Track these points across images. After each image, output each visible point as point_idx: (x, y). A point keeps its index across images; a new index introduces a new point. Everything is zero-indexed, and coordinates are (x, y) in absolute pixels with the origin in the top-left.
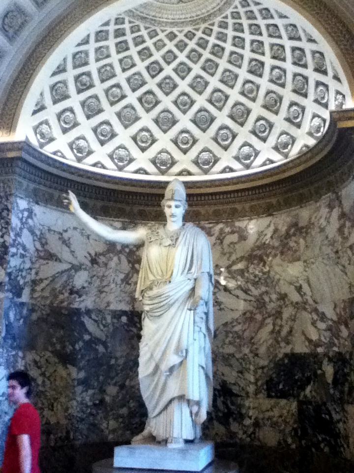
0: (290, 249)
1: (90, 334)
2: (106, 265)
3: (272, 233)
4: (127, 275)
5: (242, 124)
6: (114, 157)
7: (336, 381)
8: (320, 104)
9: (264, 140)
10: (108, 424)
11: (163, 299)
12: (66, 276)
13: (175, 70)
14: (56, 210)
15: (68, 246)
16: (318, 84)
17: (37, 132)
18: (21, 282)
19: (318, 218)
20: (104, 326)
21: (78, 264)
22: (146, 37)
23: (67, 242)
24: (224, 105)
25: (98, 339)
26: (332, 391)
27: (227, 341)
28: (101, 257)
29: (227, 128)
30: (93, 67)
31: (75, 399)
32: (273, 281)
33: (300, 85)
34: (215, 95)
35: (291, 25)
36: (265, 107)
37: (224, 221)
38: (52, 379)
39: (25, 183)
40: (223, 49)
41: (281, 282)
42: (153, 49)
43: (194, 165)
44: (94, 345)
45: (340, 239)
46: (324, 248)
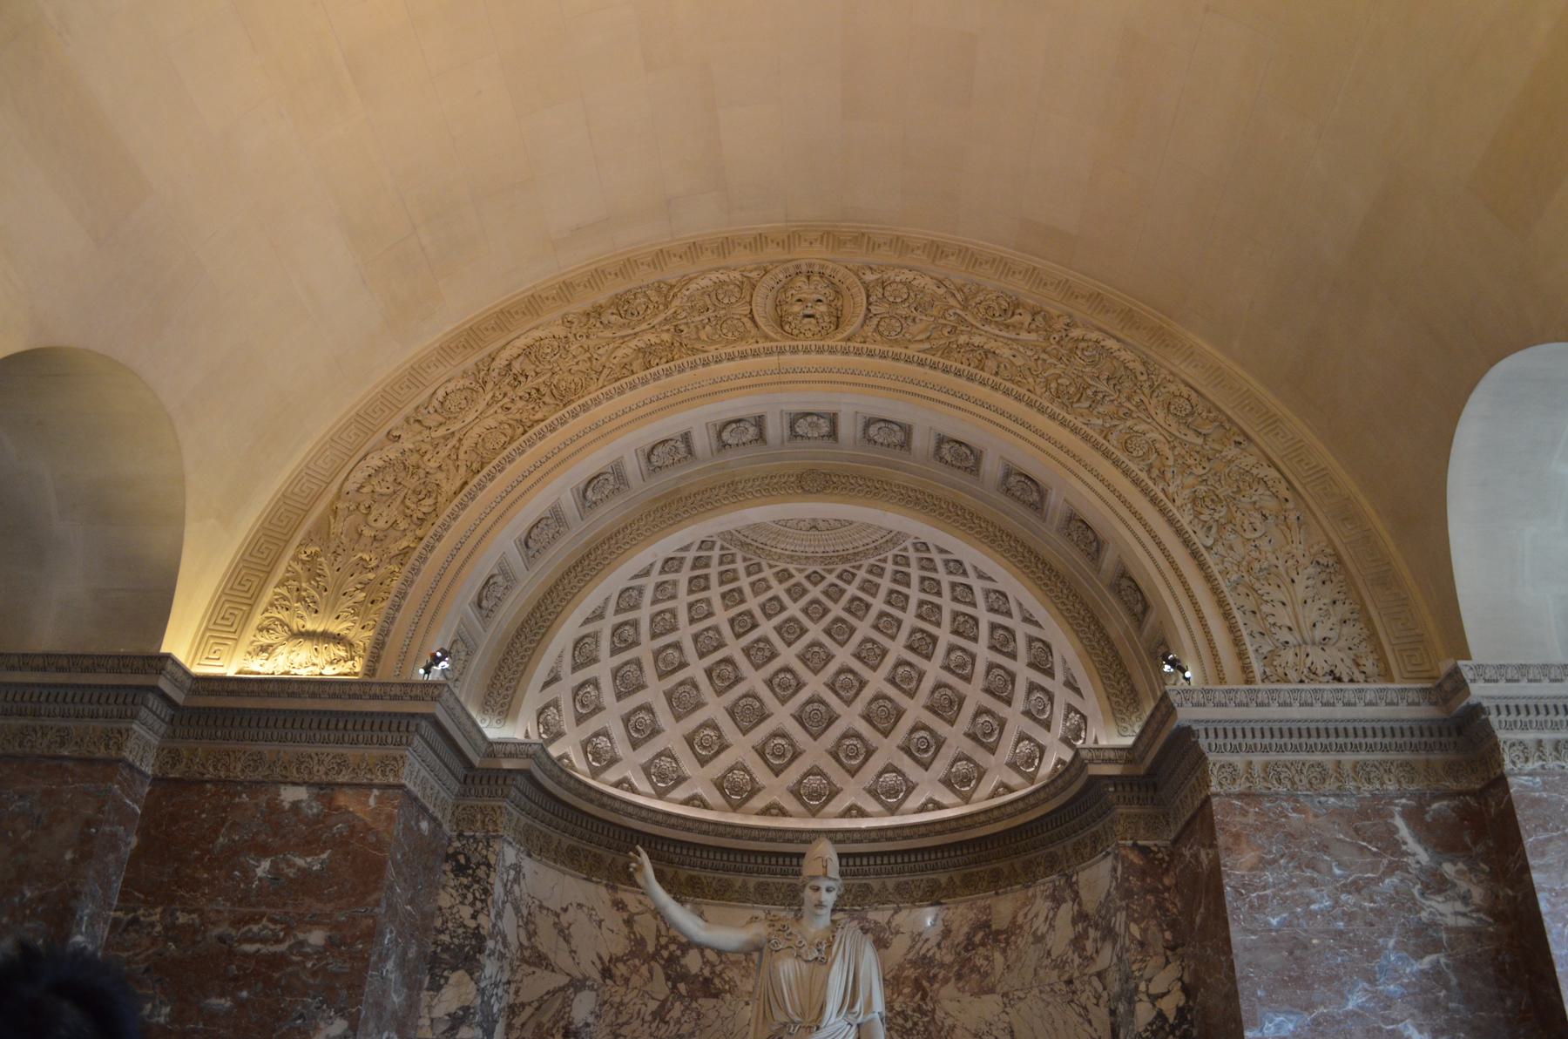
0: (975, 969)
2: (627, 981)
3: (940, 938)
4: (664, 1003)
5: (886, 734)
6: (653, 771)
8: (1034, 719)
9: (926, 766)
12: (560, 1001)
13: (778, 629)
14: (553, 868)
15: (567, 939)
16: (1033, 687)
17: (541, 720)
18: (495, 1010)
19: (1030, 917)
21: (580, 977)
22: (742, 573)
23: (567, 932)
24: (857, 694)
28: (620, 965)
29: (858, 736)
30: (644, 614)
32: (942, 1029)
33: (999, 682)
34: (842, 677)
35: (996, 591)
36: (931, 708)
37: (847, 908)
39: (516, 814)
40: (868, 606)
41: (958, 1031)
42: (747, 591)
43: (792, 797)
45: (1077, 961)
46: (1041, 972)
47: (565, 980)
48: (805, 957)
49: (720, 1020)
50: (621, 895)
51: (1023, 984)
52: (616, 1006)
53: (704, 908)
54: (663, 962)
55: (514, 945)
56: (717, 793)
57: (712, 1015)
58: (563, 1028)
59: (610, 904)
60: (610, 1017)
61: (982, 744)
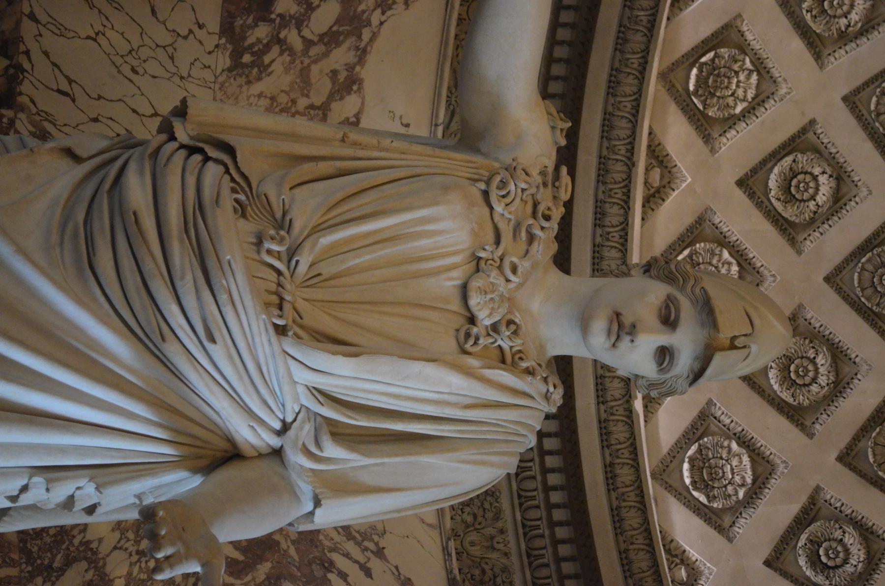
11: (190, 302)
43: (688, 220)
48: (476, 283)
49: (164, 38)
56: (705, 31)
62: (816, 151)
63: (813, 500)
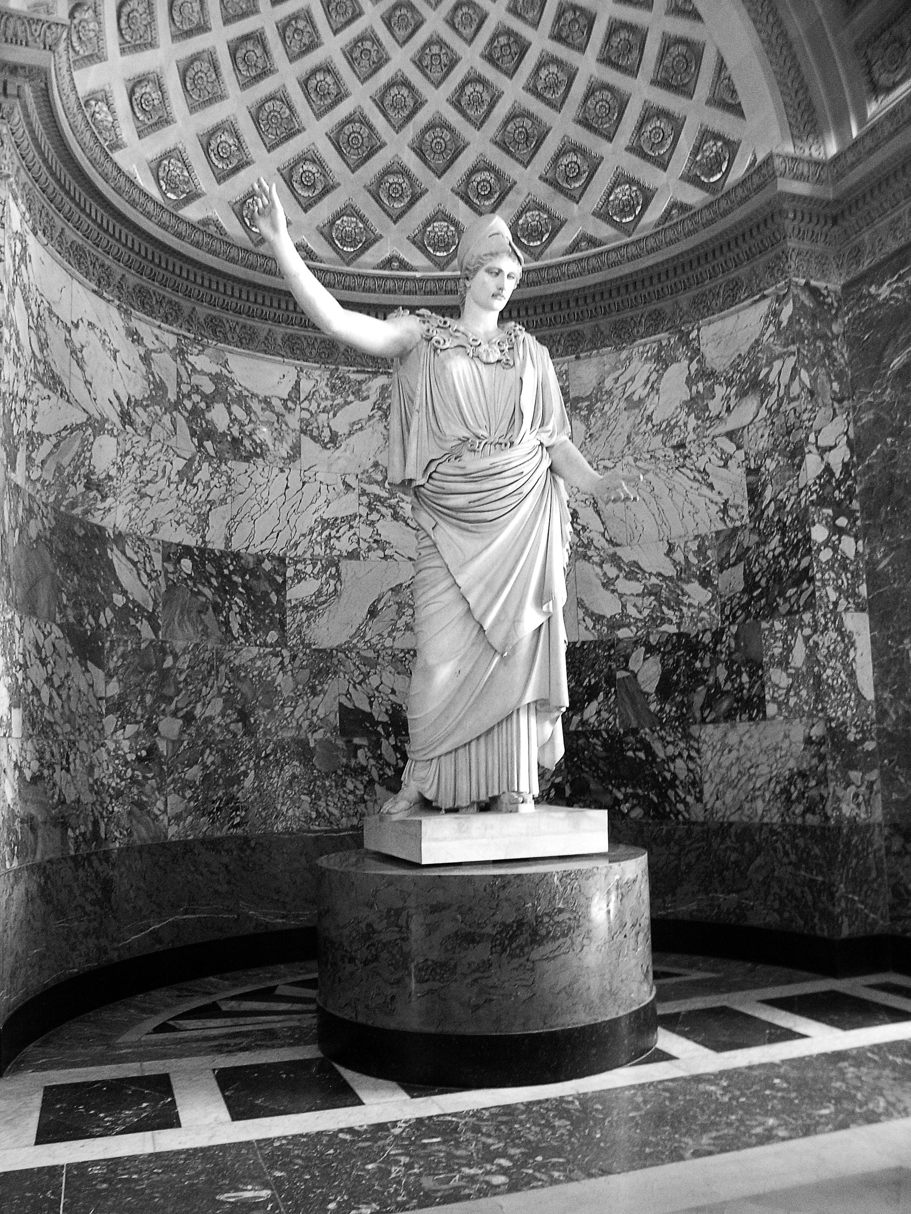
1: (124, 593)
2: (149, 430)
4: (191, 461)
6: (161, 174)
7: (665, 689)
8: (644, 156)
10: (166, 805)
15: (80, 364)
19: (622, 380)
20: (149, 575)
21: (99, 418)
23: (79, 355)
24: (409, 118)
25: (139, 606)
26: (654, 707)
27: (400, 624)
28: (139, 410)
29: (404, 172)
31: (103, 745)
36: (503, 146)
38: (64, 697)
44: (132, 622)
45: (692, 422)
46: (638, 440)
47: (82, 418)
49: (252, 487)
50: (134, 324)
51: (612, 453)
52: (138, 459)
53: (228, 355)
54: (186, 414)
55: (27, 352)
56: (236, 222)
57: (244, 480)
58: (86, 477)
59: (123, 332)
60: (133, 472)
61: (562, 190)
62: (292, 169)
63: (457, 194)
